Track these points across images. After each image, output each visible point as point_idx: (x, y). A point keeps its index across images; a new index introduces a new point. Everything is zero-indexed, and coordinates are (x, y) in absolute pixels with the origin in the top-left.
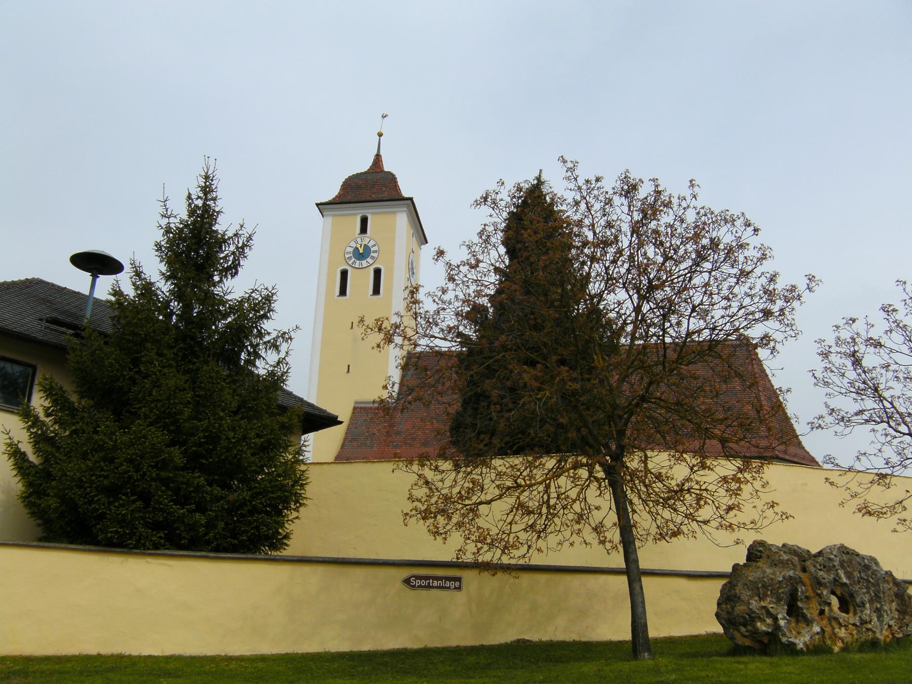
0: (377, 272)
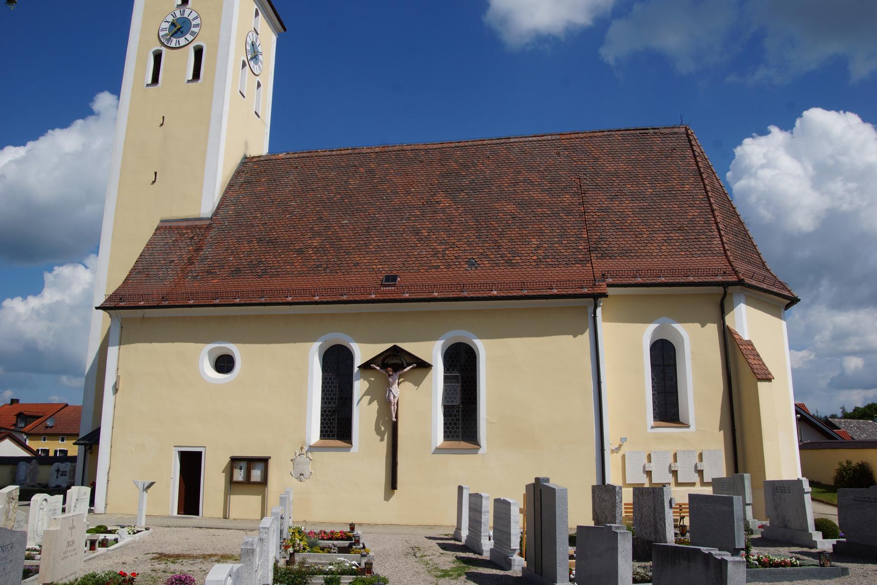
0: (199, 52)
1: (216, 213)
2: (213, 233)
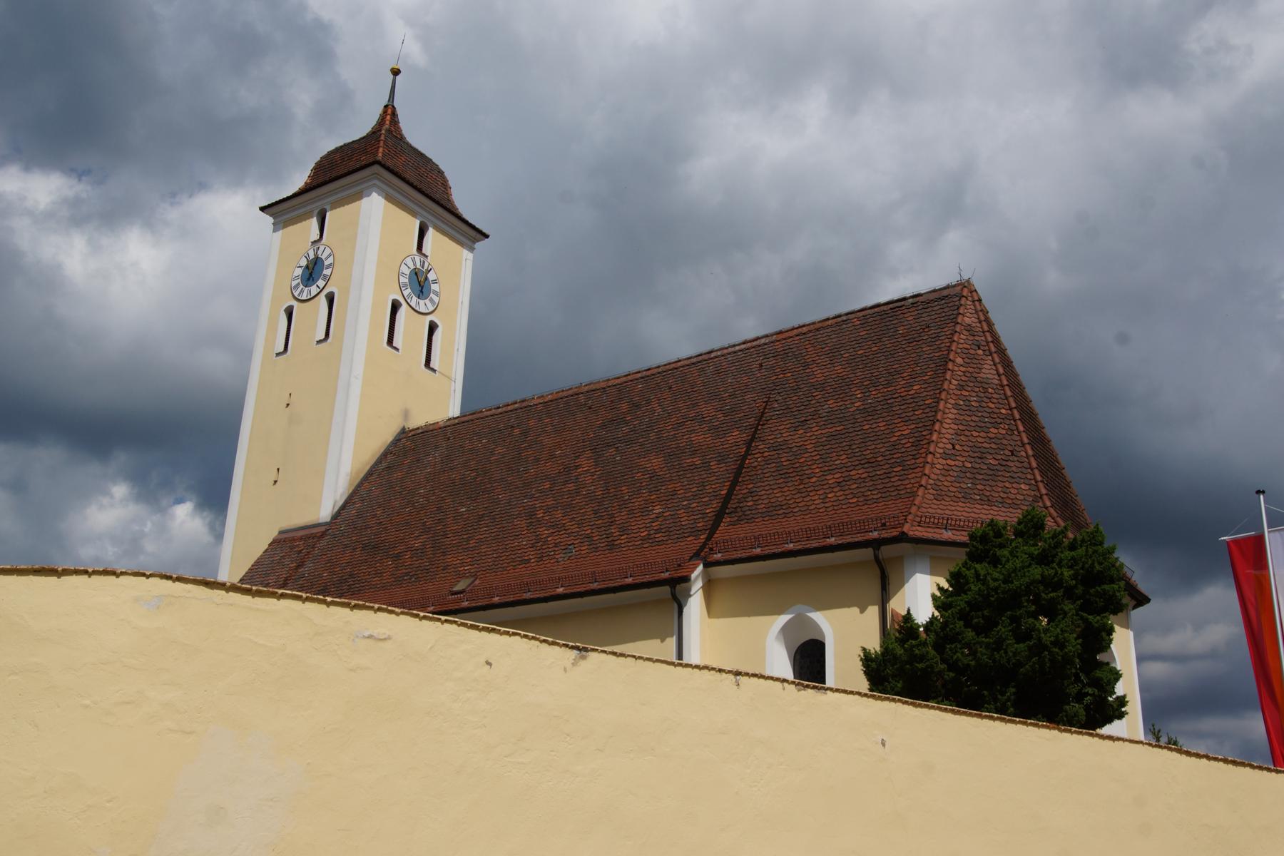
0: (331, 299)
1: (336, 516)
2: (324, 542)
